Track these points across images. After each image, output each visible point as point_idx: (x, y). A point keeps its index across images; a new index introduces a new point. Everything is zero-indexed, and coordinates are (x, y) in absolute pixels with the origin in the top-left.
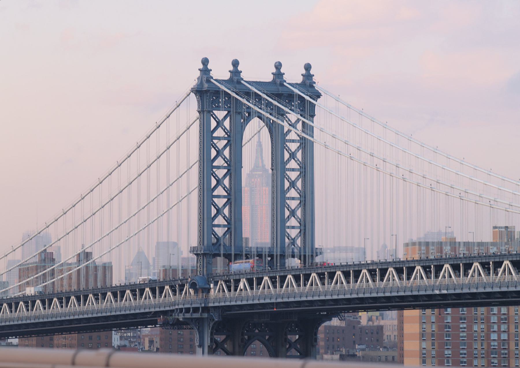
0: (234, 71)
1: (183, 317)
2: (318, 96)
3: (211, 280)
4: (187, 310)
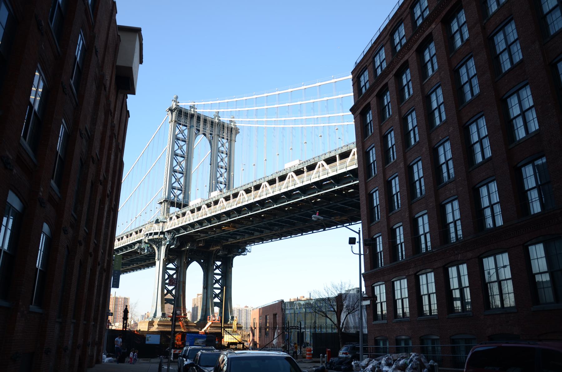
4: (151, 234)
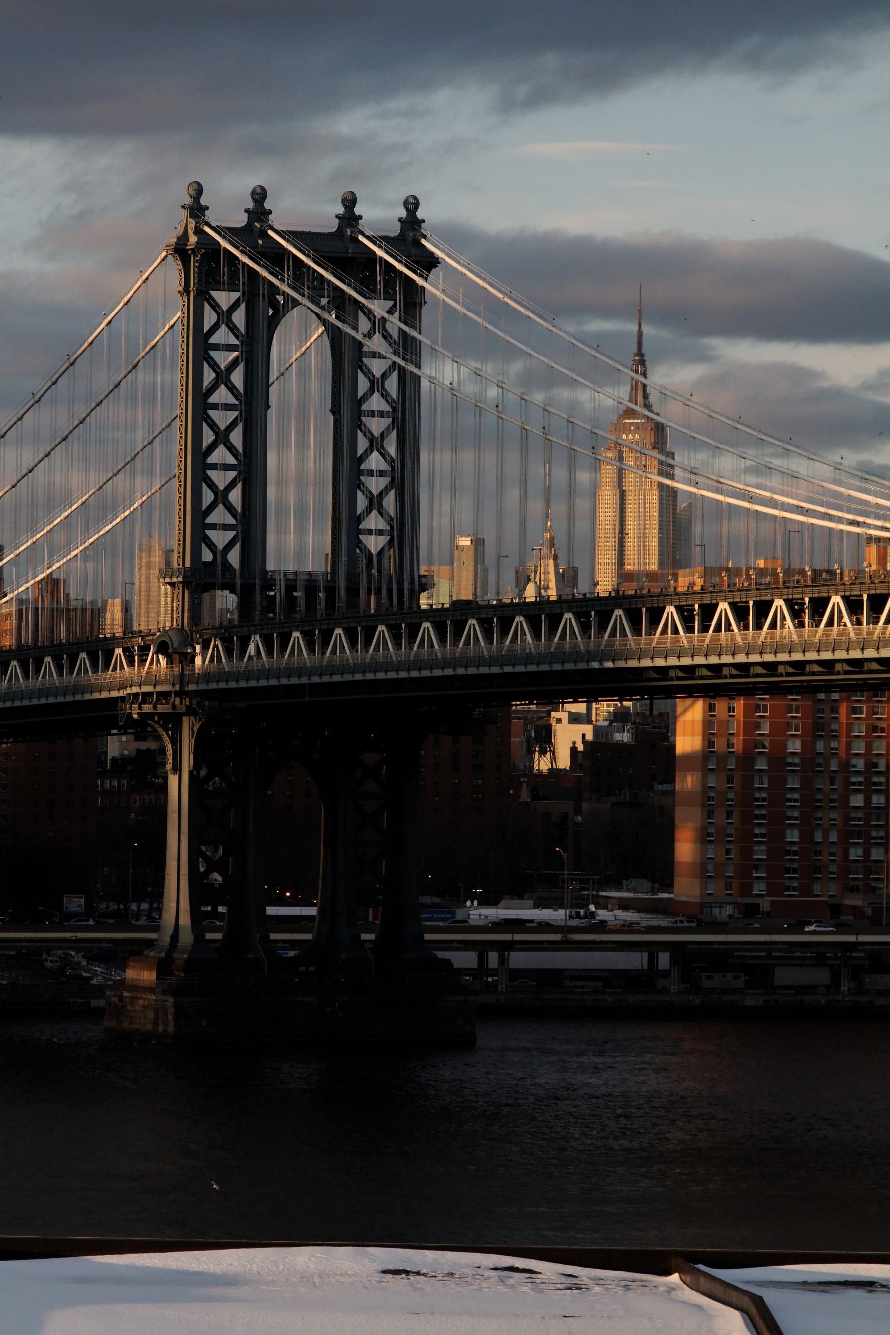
0: (409, 220)
1: (139, 711)
2: (428, 263)
3: (198, 636)
